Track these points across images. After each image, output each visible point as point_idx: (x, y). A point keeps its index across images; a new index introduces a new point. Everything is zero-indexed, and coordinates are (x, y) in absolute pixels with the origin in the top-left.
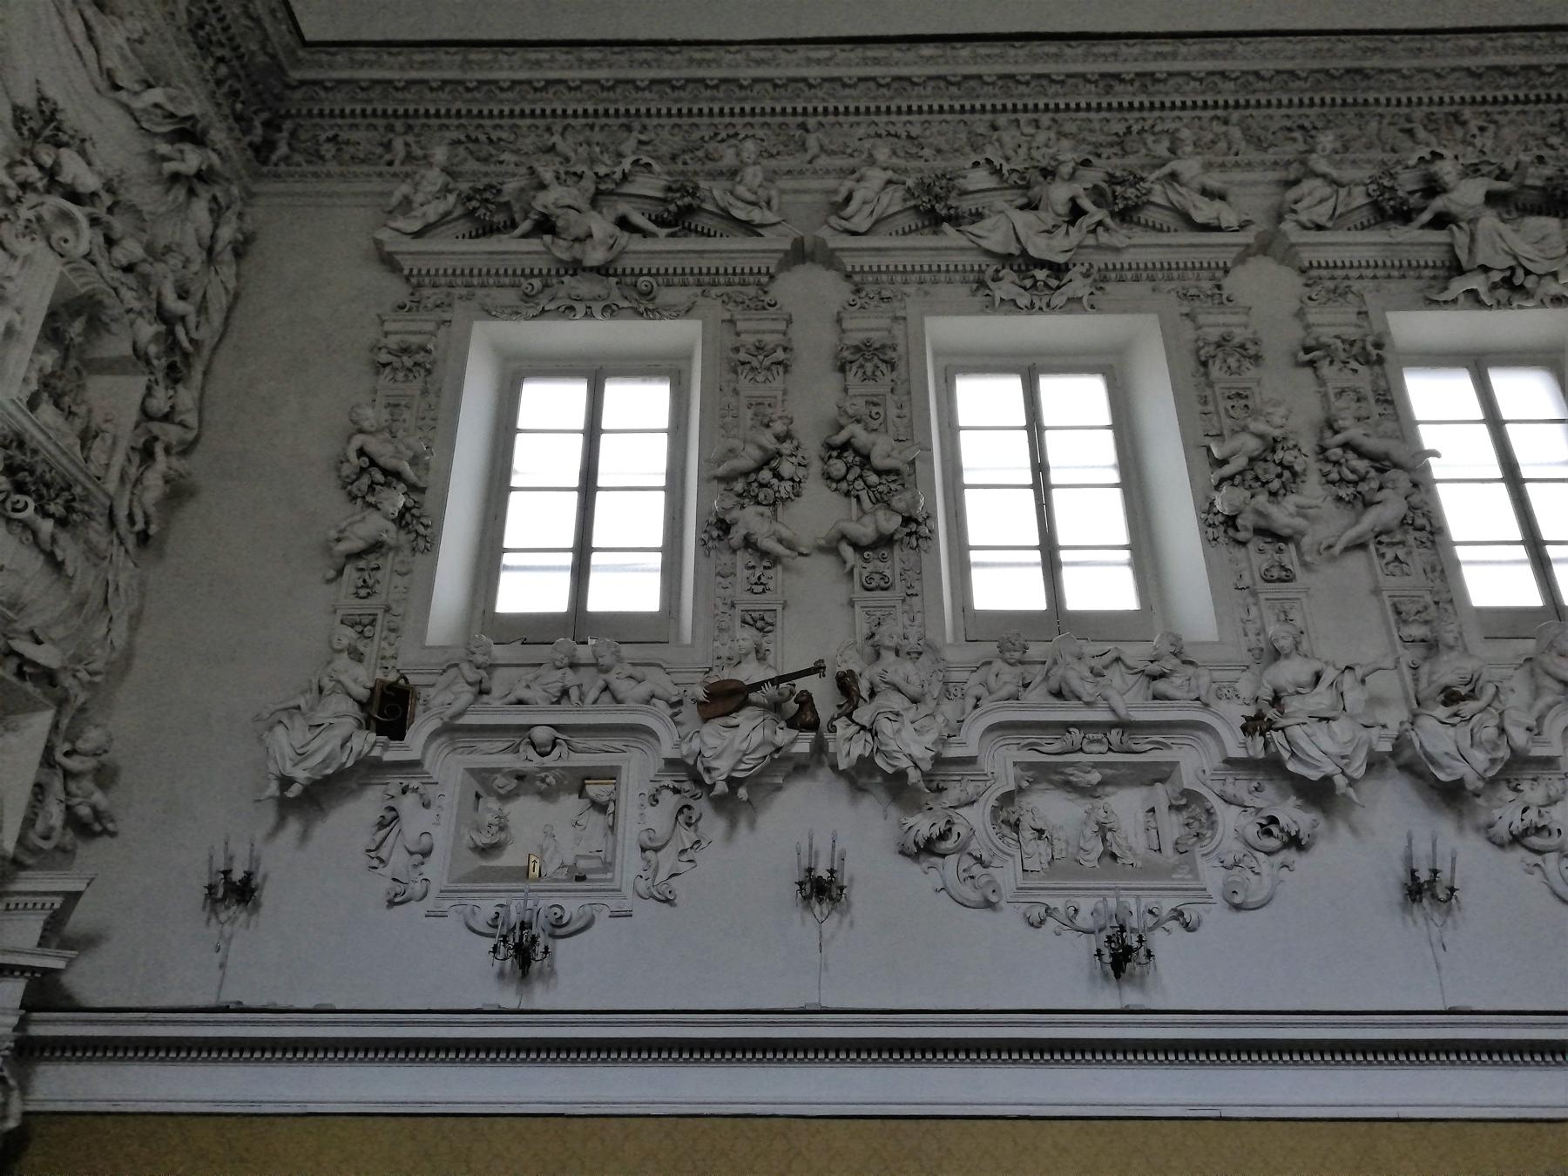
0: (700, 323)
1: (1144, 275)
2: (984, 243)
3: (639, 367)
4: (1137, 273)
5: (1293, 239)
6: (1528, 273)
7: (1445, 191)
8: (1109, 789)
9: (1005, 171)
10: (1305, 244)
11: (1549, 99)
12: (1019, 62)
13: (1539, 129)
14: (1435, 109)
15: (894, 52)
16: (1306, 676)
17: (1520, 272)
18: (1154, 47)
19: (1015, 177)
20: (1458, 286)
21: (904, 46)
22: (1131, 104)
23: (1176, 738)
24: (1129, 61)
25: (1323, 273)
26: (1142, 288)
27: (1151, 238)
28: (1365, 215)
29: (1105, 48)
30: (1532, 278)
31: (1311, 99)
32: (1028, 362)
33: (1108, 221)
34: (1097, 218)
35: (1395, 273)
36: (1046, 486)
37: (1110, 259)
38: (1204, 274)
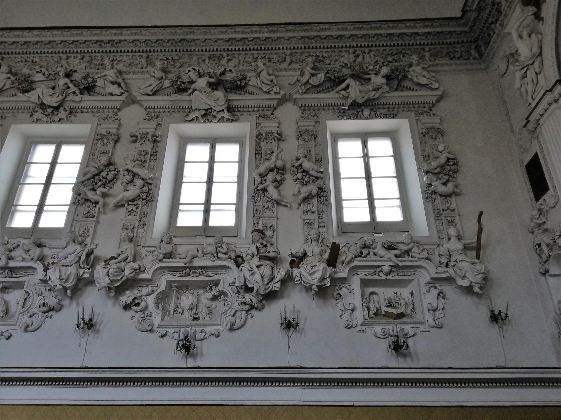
0: (171, 125)
1: (90, 110)
2: (31, 100)
3: (73, 141)
4: (88, 110)
5: (138, 99)
6: (215, 111)
7: (195, 82)
8: (10, 290)
9: (46, 74)
10: (144, 100)
11: (254, 50)
12: (68, 36)
13: (250, 60)
14: (215, 53)
15: (25, 33)
16: (71, 251)
17: (213, 110)
18: (114, 31)
19: (51, 76)
20: (192, 115)
21: (28, 31)
22: (110, 51)
23: (30, 272)
24: (106, 36)
25: (152, 110)
26: (90, 115)
27: (100, 98)
28: (171, 90)
29: (97, 31)
30: (215, 112)
31: (172, 50)
32: (59, 140)
33: (77, 92)
34: (73, 90)
35: (176, 110)
36: (208, 181)
37: (75, 105)
38: (111, 110)
